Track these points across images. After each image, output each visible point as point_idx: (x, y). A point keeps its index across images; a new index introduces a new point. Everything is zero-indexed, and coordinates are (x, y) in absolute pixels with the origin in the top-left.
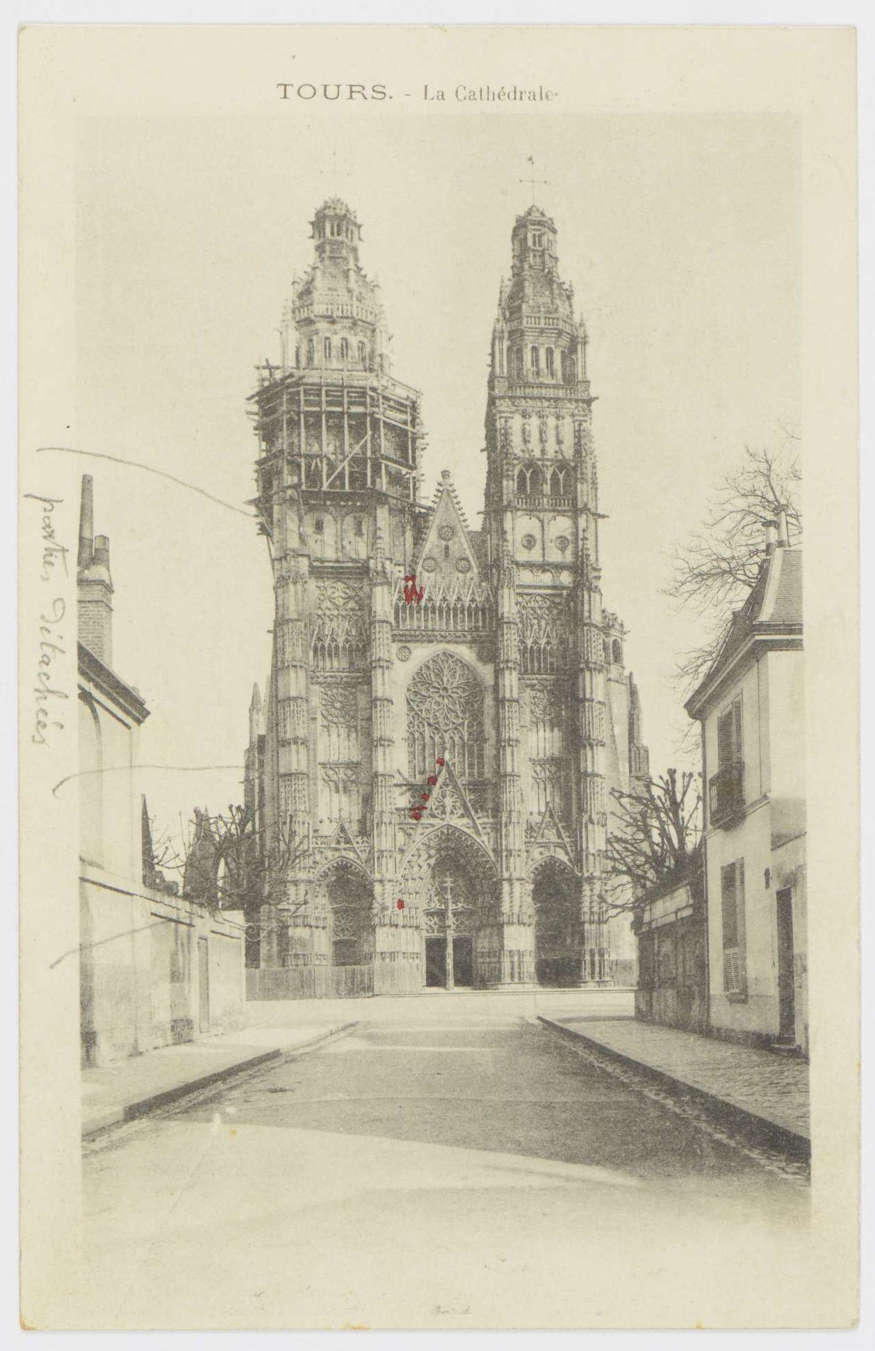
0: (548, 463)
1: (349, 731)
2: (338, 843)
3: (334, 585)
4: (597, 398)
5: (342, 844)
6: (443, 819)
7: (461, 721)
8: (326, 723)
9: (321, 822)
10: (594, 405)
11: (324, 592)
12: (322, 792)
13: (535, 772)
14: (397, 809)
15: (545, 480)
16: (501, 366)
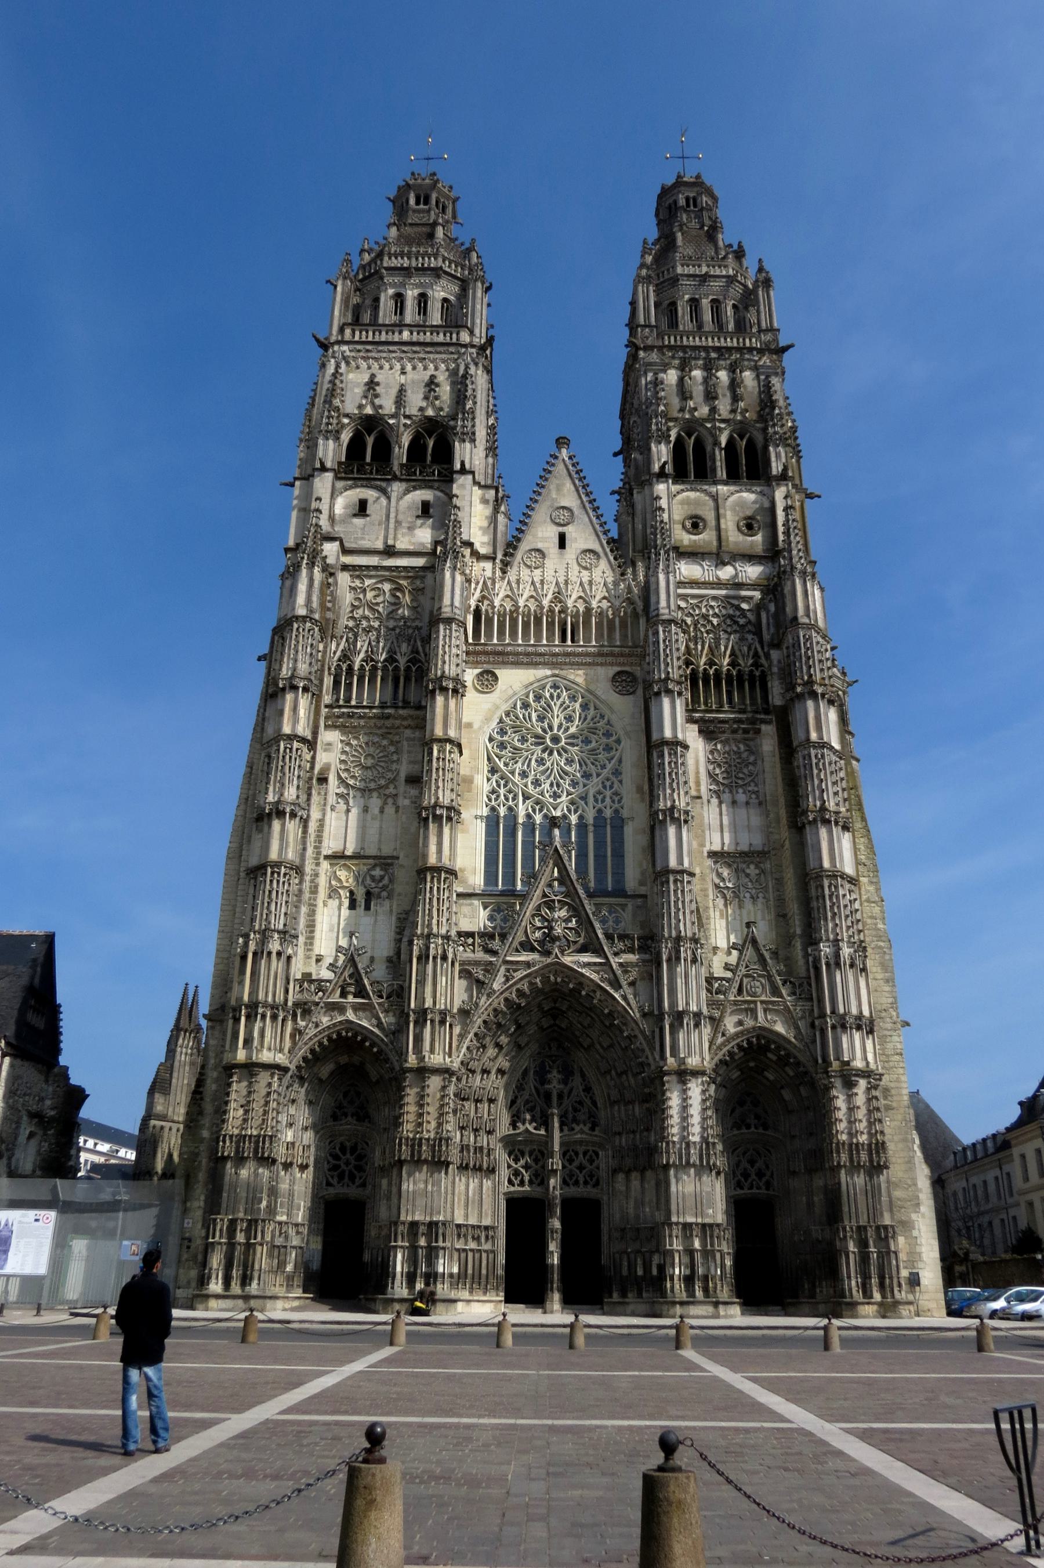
0: (723, 426)
1: (385, 803)
2: (343, 995)
3: (379, 586)
8: (342, 790)
9: (318, 961)
11: (361, 596)
12: (325, 905)
14: (460, 934)
15: (716, 443)
16: (647, 310)
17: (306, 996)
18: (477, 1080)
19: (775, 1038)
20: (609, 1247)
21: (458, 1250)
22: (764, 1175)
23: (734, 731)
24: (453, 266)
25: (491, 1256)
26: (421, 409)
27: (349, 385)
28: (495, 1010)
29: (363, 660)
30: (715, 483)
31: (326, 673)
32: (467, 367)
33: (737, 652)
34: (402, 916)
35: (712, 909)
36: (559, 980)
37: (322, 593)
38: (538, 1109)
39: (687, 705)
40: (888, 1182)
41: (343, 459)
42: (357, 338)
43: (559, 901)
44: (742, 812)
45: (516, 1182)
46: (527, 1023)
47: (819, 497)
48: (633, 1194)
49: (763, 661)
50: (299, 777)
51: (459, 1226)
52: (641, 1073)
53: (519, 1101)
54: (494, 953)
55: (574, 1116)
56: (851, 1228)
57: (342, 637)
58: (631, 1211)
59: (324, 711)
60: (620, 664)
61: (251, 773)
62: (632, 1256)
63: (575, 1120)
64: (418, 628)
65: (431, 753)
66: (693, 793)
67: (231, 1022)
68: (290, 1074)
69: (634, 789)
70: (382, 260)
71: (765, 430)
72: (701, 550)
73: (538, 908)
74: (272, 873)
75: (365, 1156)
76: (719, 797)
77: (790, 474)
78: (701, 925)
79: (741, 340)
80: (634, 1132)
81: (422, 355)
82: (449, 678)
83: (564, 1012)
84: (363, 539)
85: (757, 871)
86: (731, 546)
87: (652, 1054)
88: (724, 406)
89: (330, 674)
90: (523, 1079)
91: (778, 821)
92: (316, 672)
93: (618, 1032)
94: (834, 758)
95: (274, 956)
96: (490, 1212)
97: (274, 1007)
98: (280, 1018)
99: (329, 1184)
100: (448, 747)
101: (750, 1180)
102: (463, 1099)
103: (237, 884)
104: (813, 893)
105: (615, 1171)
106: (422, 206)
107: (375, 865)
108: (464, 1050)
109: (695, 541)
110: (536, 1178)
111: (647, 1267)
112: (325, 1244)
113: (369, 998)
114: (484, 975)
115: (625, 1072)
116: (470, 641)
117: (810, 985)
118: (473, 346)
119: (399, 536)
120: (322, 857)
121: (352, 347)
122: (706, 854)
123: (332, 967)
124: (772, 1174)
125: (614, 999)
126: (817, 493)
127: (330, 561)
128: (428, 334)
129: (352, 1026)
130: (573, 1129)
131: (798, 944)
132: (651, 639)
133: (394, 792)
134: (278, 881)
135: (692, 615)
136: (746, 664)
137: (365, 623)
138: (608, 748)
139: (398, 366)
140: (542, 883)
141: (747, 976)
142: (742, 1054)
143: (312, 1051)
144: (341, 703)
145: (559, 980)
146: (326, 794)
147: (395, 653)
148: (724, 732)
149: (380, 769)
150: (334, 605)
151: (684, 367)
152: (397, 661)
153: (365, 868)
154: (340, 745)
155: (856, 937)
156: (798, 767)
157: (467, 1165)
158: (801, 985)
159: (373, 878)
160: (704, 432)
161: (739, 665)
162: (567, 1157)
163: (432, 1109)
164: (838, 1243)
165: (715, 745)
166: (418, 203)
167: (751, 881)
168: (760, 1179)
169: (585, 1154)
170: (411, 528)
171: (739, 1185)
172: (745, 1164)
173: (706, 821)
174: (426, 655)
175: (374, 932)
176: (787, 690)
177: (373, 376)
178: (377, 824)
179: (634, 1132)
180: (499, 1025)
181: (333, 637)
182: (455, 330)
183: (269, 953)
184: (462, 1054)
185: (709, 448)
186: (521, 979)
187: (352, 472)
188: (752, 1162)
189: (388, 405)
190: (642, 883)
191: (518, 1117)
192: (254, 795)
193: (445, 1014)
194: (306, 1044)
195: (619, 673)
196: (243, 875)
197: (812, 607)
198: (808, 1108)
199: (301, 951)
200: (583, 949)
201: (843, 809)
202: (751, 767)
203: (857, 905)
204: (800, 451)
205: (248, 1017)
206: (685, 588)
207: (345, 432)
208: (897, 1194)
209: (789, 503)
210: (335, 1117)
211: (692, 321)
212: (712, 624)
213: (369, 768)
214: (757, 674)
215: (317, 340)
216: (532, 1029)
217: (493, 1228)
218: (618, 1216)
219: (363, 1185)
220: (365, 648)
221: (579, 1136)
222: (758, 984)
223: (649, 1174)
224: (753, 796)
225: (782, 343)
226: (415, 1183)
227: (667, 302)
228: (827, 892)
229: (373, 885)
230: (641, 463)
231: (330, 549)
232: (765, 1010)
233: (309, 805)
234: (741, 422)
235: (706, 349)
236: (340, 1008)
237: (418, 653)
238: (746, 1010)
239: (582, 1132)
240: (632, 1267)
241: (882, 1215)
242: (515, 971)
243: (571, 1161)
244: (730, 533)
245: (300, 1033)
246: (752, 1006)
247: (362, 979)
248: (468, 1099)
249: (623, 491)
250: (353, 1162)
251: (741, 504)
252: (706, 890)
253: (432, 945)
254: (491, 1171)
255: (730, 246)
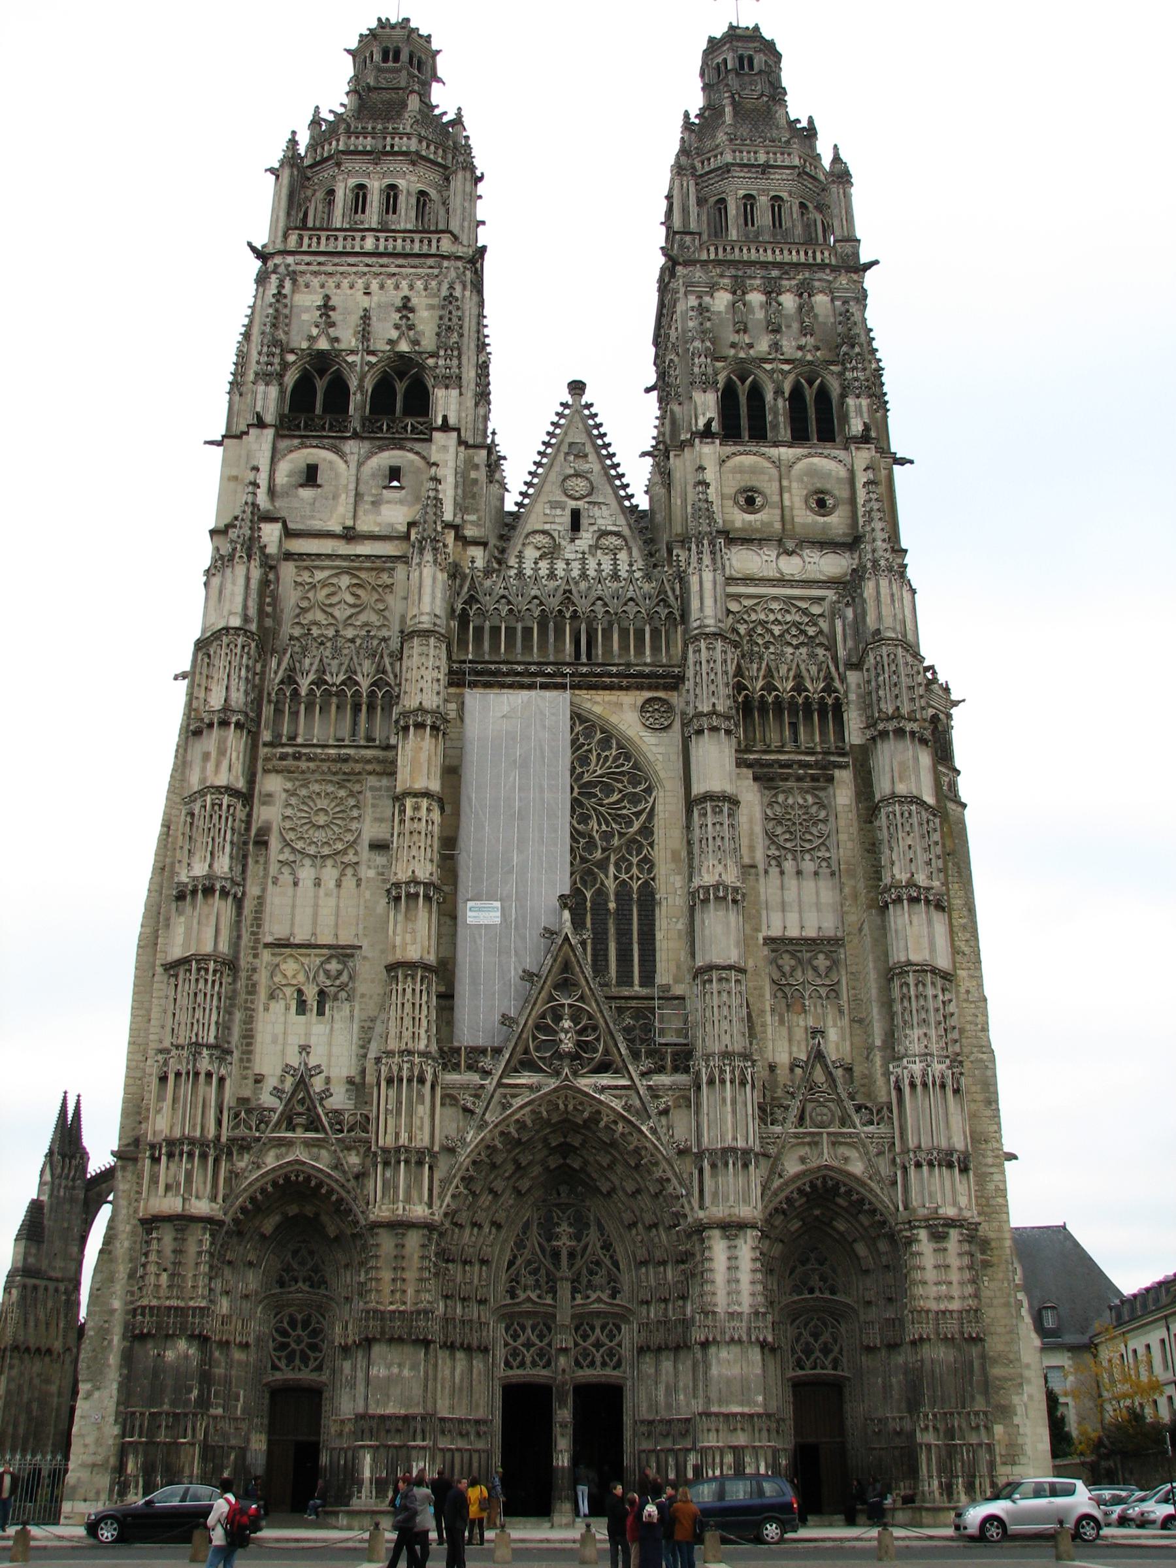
0: (786, 367)
1: (342, 874)
3: (334, 581)
4: (876, 263)
5: (299, 1130)
6: (557, 1073)
7: (598, 855)
9: (257, 1081)
10: (870, 280)
11: (310, 595)
13: (779, 967)
17: (242, 1131)
18: (467, 1236)
19: (846, 1180)
20: (633, 1444)
21: (442, 1450)
22: (831, 1351)
23: (799, 779)
24: (432, 148)
25: (483, 1456)
26: (391, 342)
27: (295, 310)
28: (488, 1147)
29: (312, 683)
30: (776, 444)
31: (265, 702)
32: (451, 287)
33: (805, 673)
34: (367, 1025)
35: (768, 1014)
36: (571, 1107)
37: (261, 595)
38: (543, 1271)
39: (739, 743)
40: (983, 1356)
41: (286, 411)
42: (305, 248)
43: (570, 1006)
44: (809, 885)
45: (515, 1364)
46: (530, 1163)
47: (911, 462)
48: (664, 1377)
49: (837, 684)
50: (232, 842)
51: (442, 1420)
52: (675, 1226)
53: (519, 1261)
54: (486, 1073)
55: (589, 1281)
56: (935, 1415)
57: (285, 650)
58: (661, 1398)
59: (263, 751)
60: (650, 688)
61: (168, 834)
62: (662, 1456)
63: (590, 1285)
64: (384, 640)
65: (403, 811)
66: (746, 861)
67: (148, 1162)
68: (225, 1229)
69: (669, 855)
70: (338, 140)
71: (841, 374)
72: (758, 536)
73: (543, 1016)
74: (199, 970)
75: (322, 1331)
76: (779, 865)
77: (873, 434)
78: (752, 1035)
79: (810, 253)
80: (666, 1301)
81: (393, 270)
82: (427, 712)
83: (577, 1148)
84: (312, 517)
85: (828, 963)
86: (798, 530)
87: (689, 1202)
88: (788, 346)
89: (269, 702)
90: (524, 1233)
91: (855, 897)
92: (252, 702)
93: (646, 1174)
94: (925, 815)
95: (202, 1077)
96: (482, 1403)
97: (203, 1143)
98: (211, 1160)
99: (275, 1367)
100: (424, 803)
101: (812, 1359)
102: (447, 1261)
103: (152, 983)
104: (896, 993)
105: (642, 1350)
106: (390, 64)
107: (331, 957)
108: (448, 1199)
109: (750, 522)
110: (541, 1359)
111: (680, 1469)
112: (270, 1443)
113: (326, 1133)
114: (474, 1103)
115: (655, 1225)
116: (454, 657)
117: (891, 1111)
118: (459, 258)
119: (360, 513)
120: (261, 946)
121: (298, 257)
122: (761, 941)
123: (277, 1092)
124: (841, 1349)
125: (641, 1132)
126: (908, 457)
127: (272, 549)
128: (399, 241)
129: (304, 1168)
130: (588, 1297)
131: (878, 1061)
132: (691, 657)
133: (355, 860)
134: (206, 980)
135: (746, 622)
136: (814, 688)
137: (315, 631)
138: (635, 799)
139: (360, 283)
140: (549, 983)
141: (811, 1101)
142: (804, 1199)
143: (253, 1199)
144: (284, 740)
145: (571, 1107)
146: (266, 863)
147: (355, 673)
148: (786, 780)
149: (336, 829)
150: (274, 609)
151: (739, 289)
152: (357, 683)
153: (318, 961)
154: (284, 795)
155: (950, 1049)
156: (880, 829)
157: (452, 1343)
158: (879, 1111)
159: (327, 974)
160: (764, 377)
161: (807, 690)
162: (580, 1332)
163: (411, 1275)
164: (918, 1434)
165: (775, 795)
166: (385, 59)
167: (820, 976)
168: (826, 1356)
169: (603, 1328)
170: (376, 504)
171: (800, 1365)
172: (806, 1336)
173: (763, 898)
174: (396, 676)
175: (330, 1044)
176: (867, 727)
177: (327, 297)
178: (332, 902)
179: (666, 1301)
180: (494, 1166)
181: (274, 651)
182: (434, 237)
183: (197, 1074)
184: (445, 1205)
185: (769, 397)
186: (521, 1107)
187: (298, 427)
188: (816, 1336)
189: (348, 338)
190: (677, 980)
191: (518, 1283)
192: (173, 864)
193: (423, 1153)
194: (245, 1190)
195: (649, 701)
196: (159, 970)
197: (900, 616)
198: (887, 1267)
199: (235, 1069)
200: (603, 1067)
201: (936, 884)
202: (820, 826)
203: (952, 1008)
204: (887, 402)
205: (170, 1156)
206: (737, 585)
207: (289, 373)
208: (996, 1371)
209: (871, 476)
210: (282, 1284)
211: (746, 224)
212: (772, 634)
213: (323, 827)
214: (830, 701)
215: (253, 249)
216: (537, 1170)
217: (485, 1422)
218: (644, 1406)
219: (319, 1368)
220: (314, 667)
221: (596, 1305)
222: (825, 1110)
223: (682, 1354)
224: (824, 864)
225: (864, 259)
226: (389, 1367)
227: (712, 200)
228: (912, 993)
229: (328, 983)
230: (678, 415)
231: (271, 533)
232: (834, 1144)
233: (244, 879)
234: (810, 363)
235: (764, 265)
236: (289, 1144)
237: (384, 672)
238: (809, 1144)
239: (599, 1300)
240: (662, 1469)
241: (973, 1398)
242: (514, 1096)
243: (585, 1337)
244: (796, 512)
245: (237, 1175)
246: (816, 1139)
247: (315, 1107)
248: (453, 1261)
249: (656, 453)
250: (306, 1340)
251: (812, 472)
252: (762, 988)
253: (406, 1066)
254: (485, 1350)
255: (798, 121)
